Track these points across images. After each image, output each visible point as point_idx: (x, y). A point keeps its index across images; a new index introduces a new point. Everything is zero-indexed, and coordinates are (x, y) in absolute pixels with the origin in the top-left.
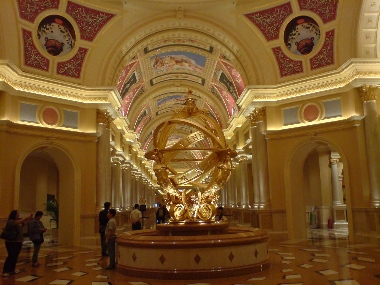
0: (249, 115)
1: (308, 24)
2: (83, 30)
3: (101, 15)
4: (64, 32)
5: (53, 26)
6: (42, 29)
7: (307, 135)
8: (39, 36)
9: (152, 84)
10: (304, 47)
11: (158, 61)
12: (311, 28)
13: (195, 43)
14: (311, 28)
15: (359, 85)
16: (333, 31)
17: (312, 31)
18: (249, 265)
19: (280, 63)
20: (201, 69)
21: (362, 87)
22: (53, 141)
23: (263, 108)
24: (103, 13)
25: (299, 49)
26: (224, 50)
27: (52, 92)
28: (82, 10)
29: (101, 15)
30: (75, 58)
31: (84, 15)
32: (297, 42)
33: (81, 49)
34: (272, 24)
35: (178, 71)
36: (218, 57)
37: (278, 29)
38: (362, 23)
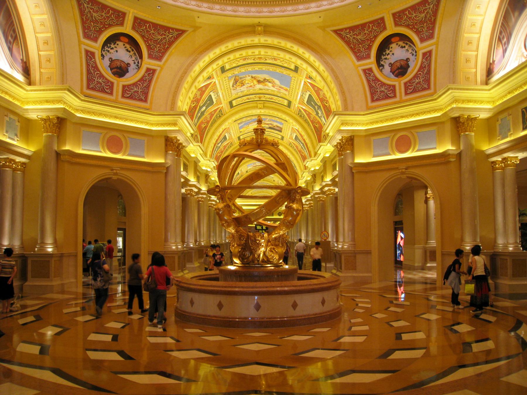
0: (336, 144)
1: (404, 43)
2: (151, 49)
3: (171, 31)
4: (130, 52)
5: (118, 44)
6: (106, 48)
7: (397, 168)
8: (103, 56)
9: (231, 106)
10: (398, 69)
11: (238, 81)
12: (407, 47)
13: (279, 61)
14: (407, 47)
15: (457, 115)
16: (430, 52)
17: (407, 50)
18: (314, 315)
19: (370, 87)
20: (286, 90)
21: (459, 117)
22: (118, 172)
23: (351, 136)
24: (173, 29)
25: (392, 72)
26: (310, 69)
27: (116, 117)
28: (149, 26)
29: (171, 31)
30: (142, 80)
31: (153, 32)
32: (390, 63)
33: (148, 70)
34: (363, 41)
35: (260, 92)
36: (304, 77)
37: (370, 48)
38: (463, 44)
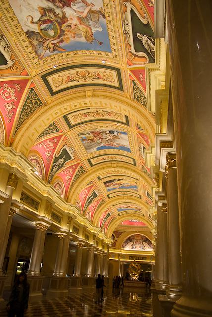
13: (112, 116)
